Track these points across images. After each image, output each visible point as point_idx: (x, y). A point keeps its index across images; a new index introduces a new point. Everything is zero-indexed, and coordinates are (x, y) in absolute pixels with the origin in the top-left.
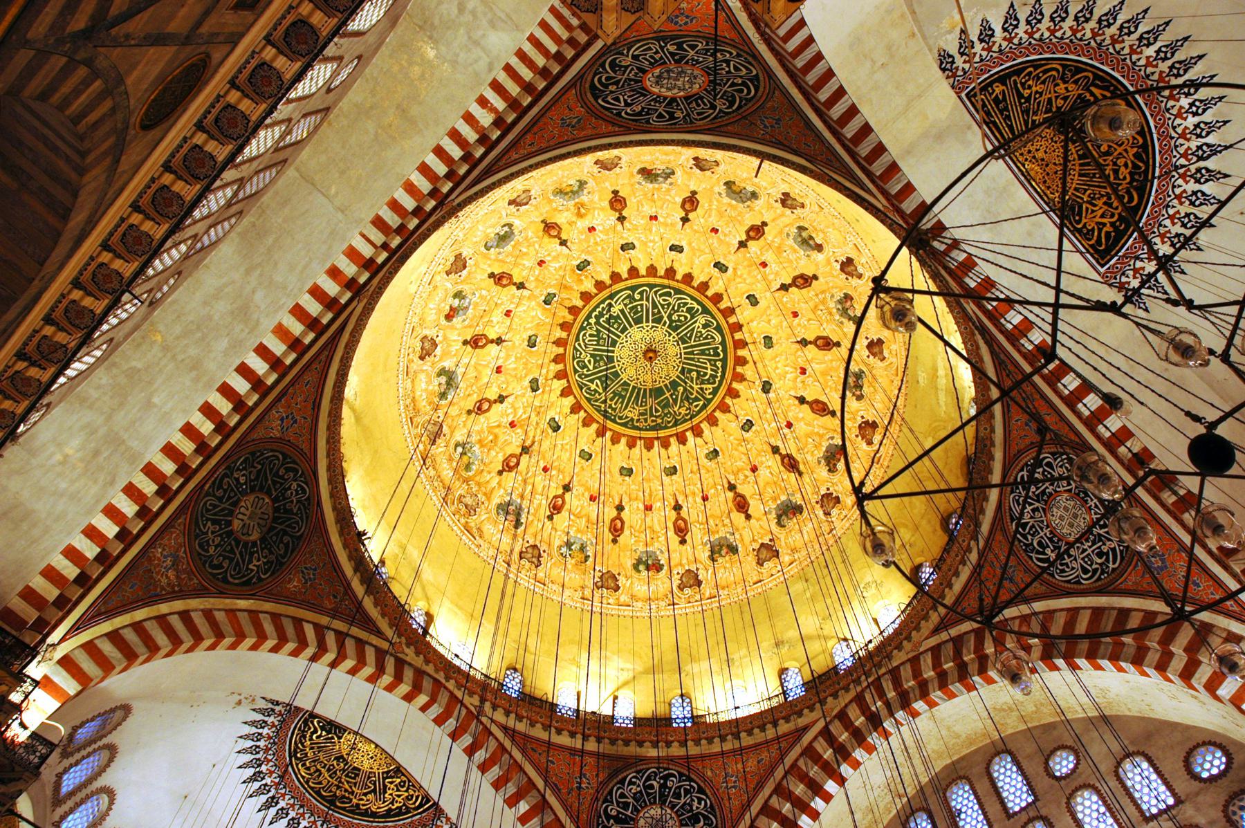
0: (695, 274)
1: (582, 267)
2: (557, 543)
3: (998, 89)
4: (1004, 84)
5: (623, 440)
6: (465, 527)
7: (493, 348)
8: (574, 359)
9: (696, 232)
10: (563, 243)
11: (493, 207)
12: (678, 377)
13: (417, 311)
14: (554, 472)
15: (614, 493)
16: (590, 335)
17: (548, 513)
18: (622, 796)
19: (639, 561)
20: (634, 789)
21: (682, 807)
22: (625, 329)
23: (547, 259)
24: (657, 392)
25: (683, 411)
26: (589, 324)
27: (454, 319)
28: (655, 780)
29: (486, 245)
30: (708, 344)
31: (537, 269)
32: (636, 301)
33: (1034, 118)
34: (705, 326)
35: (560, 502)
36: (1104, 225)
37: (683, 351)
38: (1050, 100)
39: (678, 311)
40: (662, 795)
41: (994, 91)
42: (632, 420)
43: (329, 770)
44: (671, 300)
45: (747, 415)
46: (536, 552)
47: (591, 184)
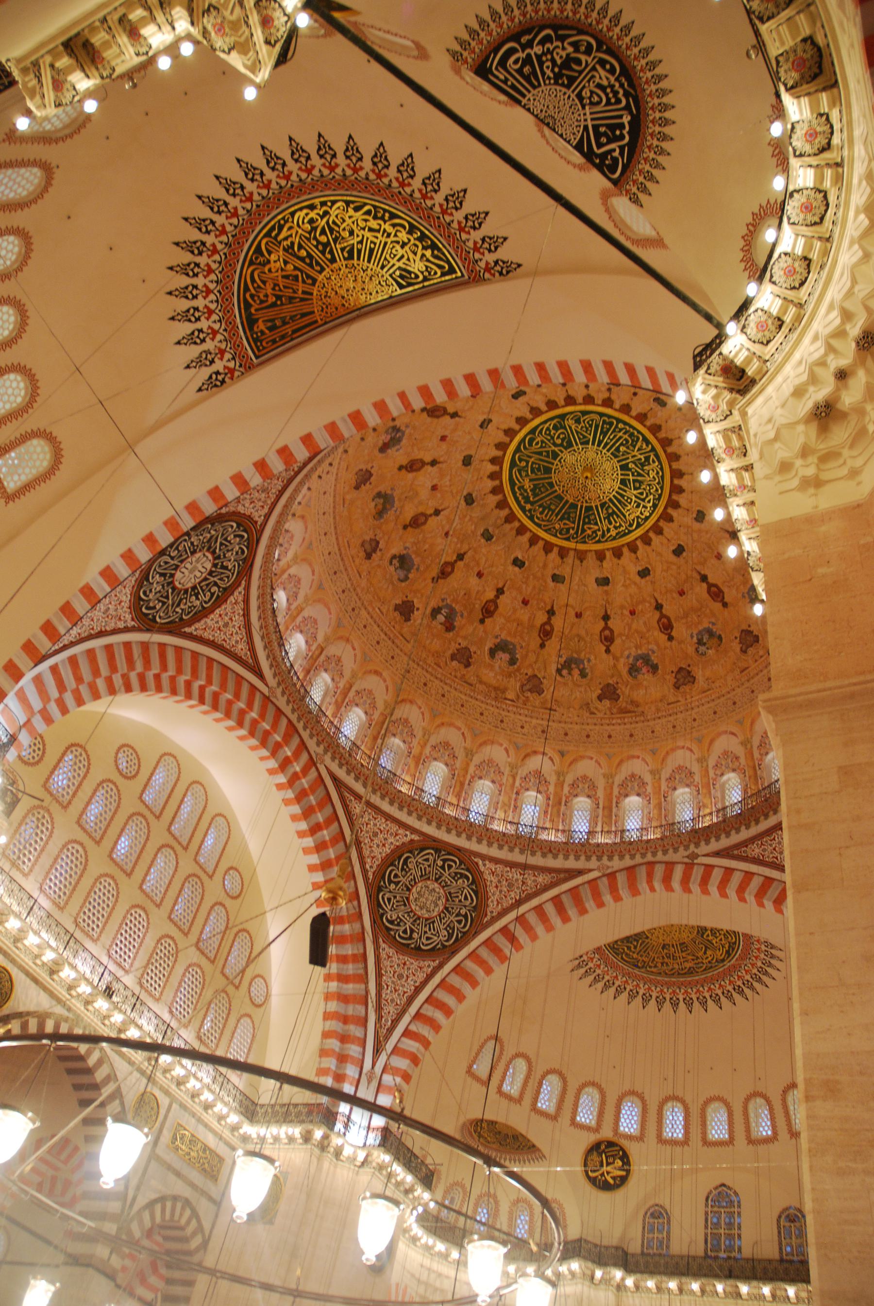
0: (519, 414)
1: (469, 500)
2: (691, 650)
3: (261, 326)
4: (257, 320)
5: (651, 534)
7: (503, 600)
8: (556, 536)
9: (472, 408)
10: (437, 512)
11: (364, 574)
13: (424, 655)
15: (689, 573)
16: (541, 513)
22: (551, 485)
24: (623, 482)
25: (652, 474)
26: (530, 511)
29: (402, 581)
30: (597, 427)
32: (527, 466)
33: (300, 292)
34: (578, 421)
35: (664, 620)
36: (423, 255)
38: (284, 277)
39: (553, 438)
41: (262, 332)
42: (638, 517)
43: (669, 957)
44: (539, 439)
47: (382, 488)
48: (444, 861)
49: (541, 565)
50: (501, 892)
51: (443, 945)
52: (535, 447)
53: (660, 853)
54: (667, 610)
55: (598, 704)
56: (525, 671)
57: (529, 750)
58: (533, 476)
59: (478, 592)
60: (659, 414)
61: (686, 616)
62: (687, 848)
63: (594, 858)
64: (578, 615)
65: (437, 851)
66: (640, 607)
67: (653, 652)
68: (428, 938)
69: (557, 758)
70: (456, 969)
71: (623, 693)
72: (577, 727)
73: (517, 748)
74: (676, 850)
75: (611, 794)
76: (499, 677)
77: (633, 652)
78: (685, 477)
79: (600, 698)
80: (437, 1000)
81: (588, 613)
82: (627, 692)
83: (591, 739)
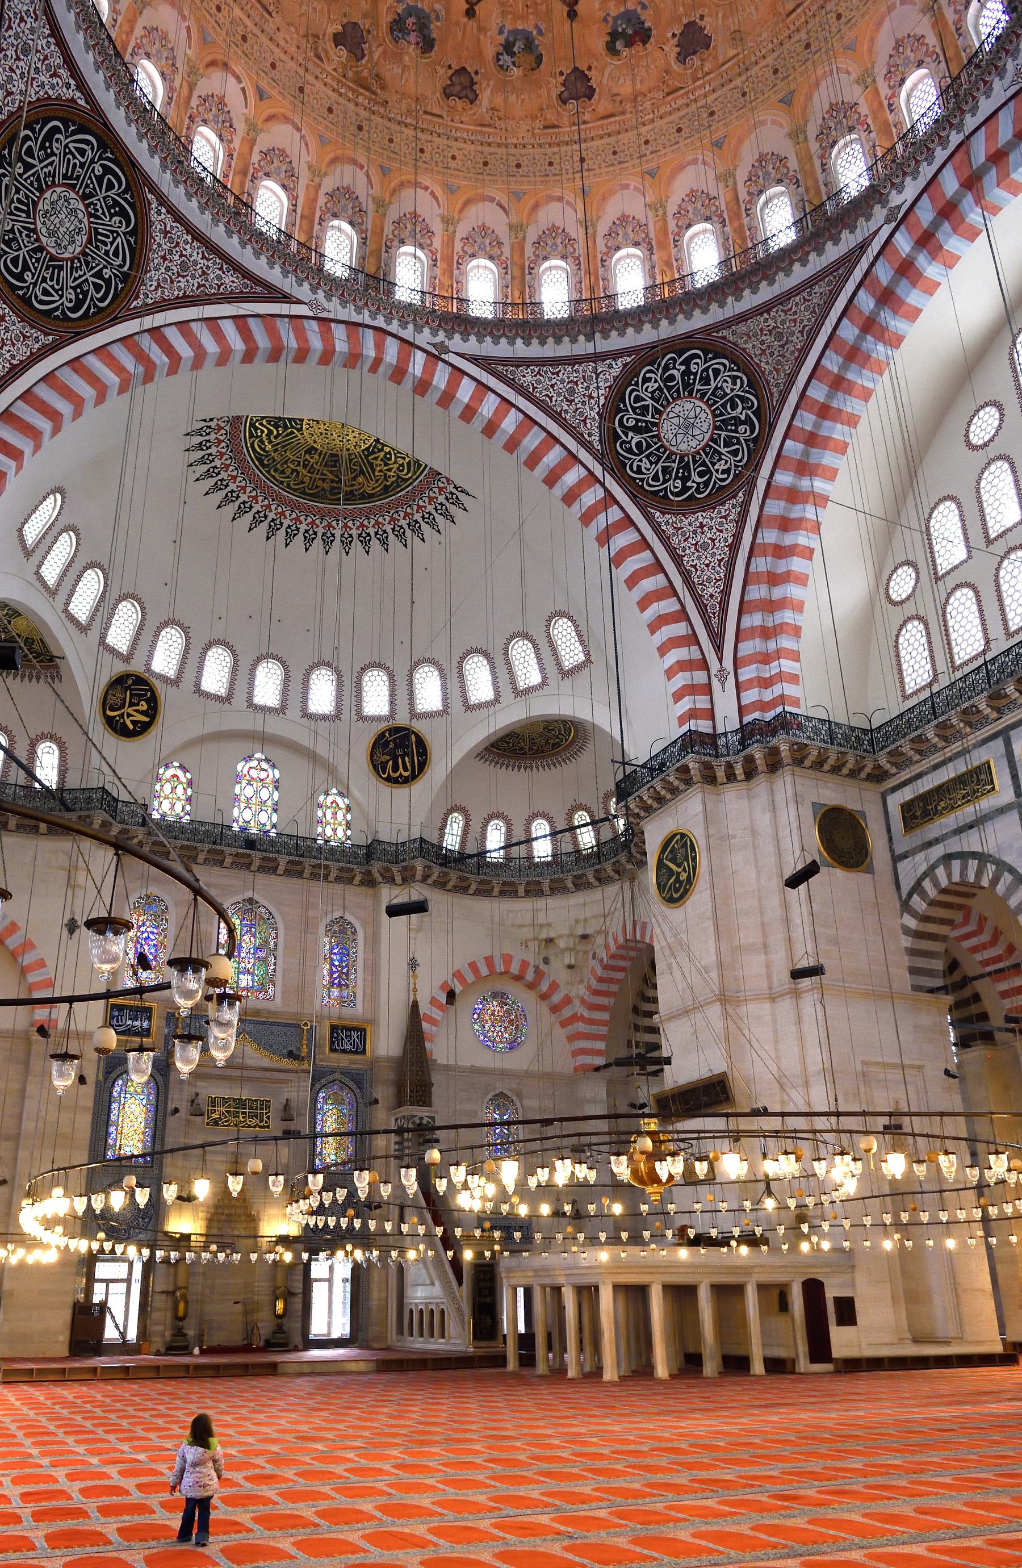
2: (490, 51)
6: (355, 82)
18: (638, 399)
20: (652, 386)
21: (713, 394)
28: (674, 368)
40: (686, 385)
46: (464, 79)
48: (107, 170)
50: (168, 269)
51: (63, 312)
53: (395, 322)
55: (330, 45)
57: (220, 57)
62: (434, 333)
63: (306, 285)
65: (103, 146)
67: (438, 19)
68: (46, 293)
70: (74, 363)
71: (371, 53)
73: (204, 41)
74: (419, 329)
75: (315, 200)
79: (338, 39)
80: (43, 402)
82: (376, 56)
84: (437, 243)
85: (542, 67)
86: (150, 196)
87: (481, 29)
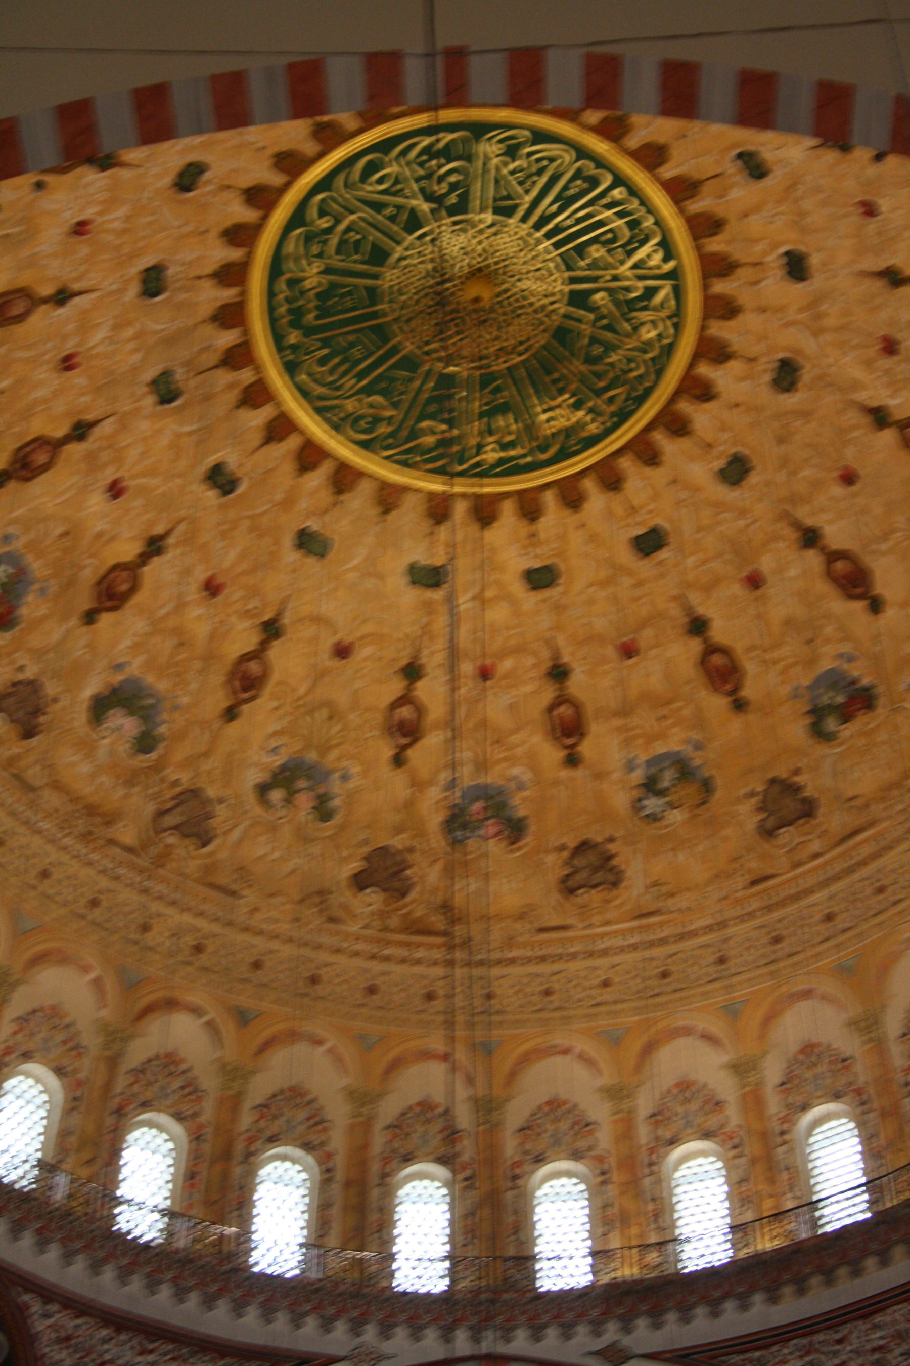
2: (621, 800)
10: (62, 297)
12: (573, 280)
14: (507, 664)
16: (322, 361)
17: (562, 754)
19: (817, 714)
22: (373, 295)
23: (69, 347)
25: (646, 333)
26: (294, 348)
27: (24, 611)
31: (78, 378)
34: (512, 152)
37: (526, 226)
42: (568, 432)
45: (774, 246)
46: (592, 858)
49: (279, 497)
52: (371, 189)
54: (577, 684)
56: (172, 774)
58: (336, 262)
59: (99, 535)
60: (735, 194)
61: (625, 711)
64: (342, 651)
66: (507, 664)
67: (521, 787)
69: (228, 1028)
72: (288, 950)
76: (105, 779)
77: (467, 777)
78: (734, 365)
79: (360, 882)
81: (367, 651)
83: (320, 990)
84: (604, 1138)
85: (718, 795)
86: (26, 1297)
87: (599, 776)
